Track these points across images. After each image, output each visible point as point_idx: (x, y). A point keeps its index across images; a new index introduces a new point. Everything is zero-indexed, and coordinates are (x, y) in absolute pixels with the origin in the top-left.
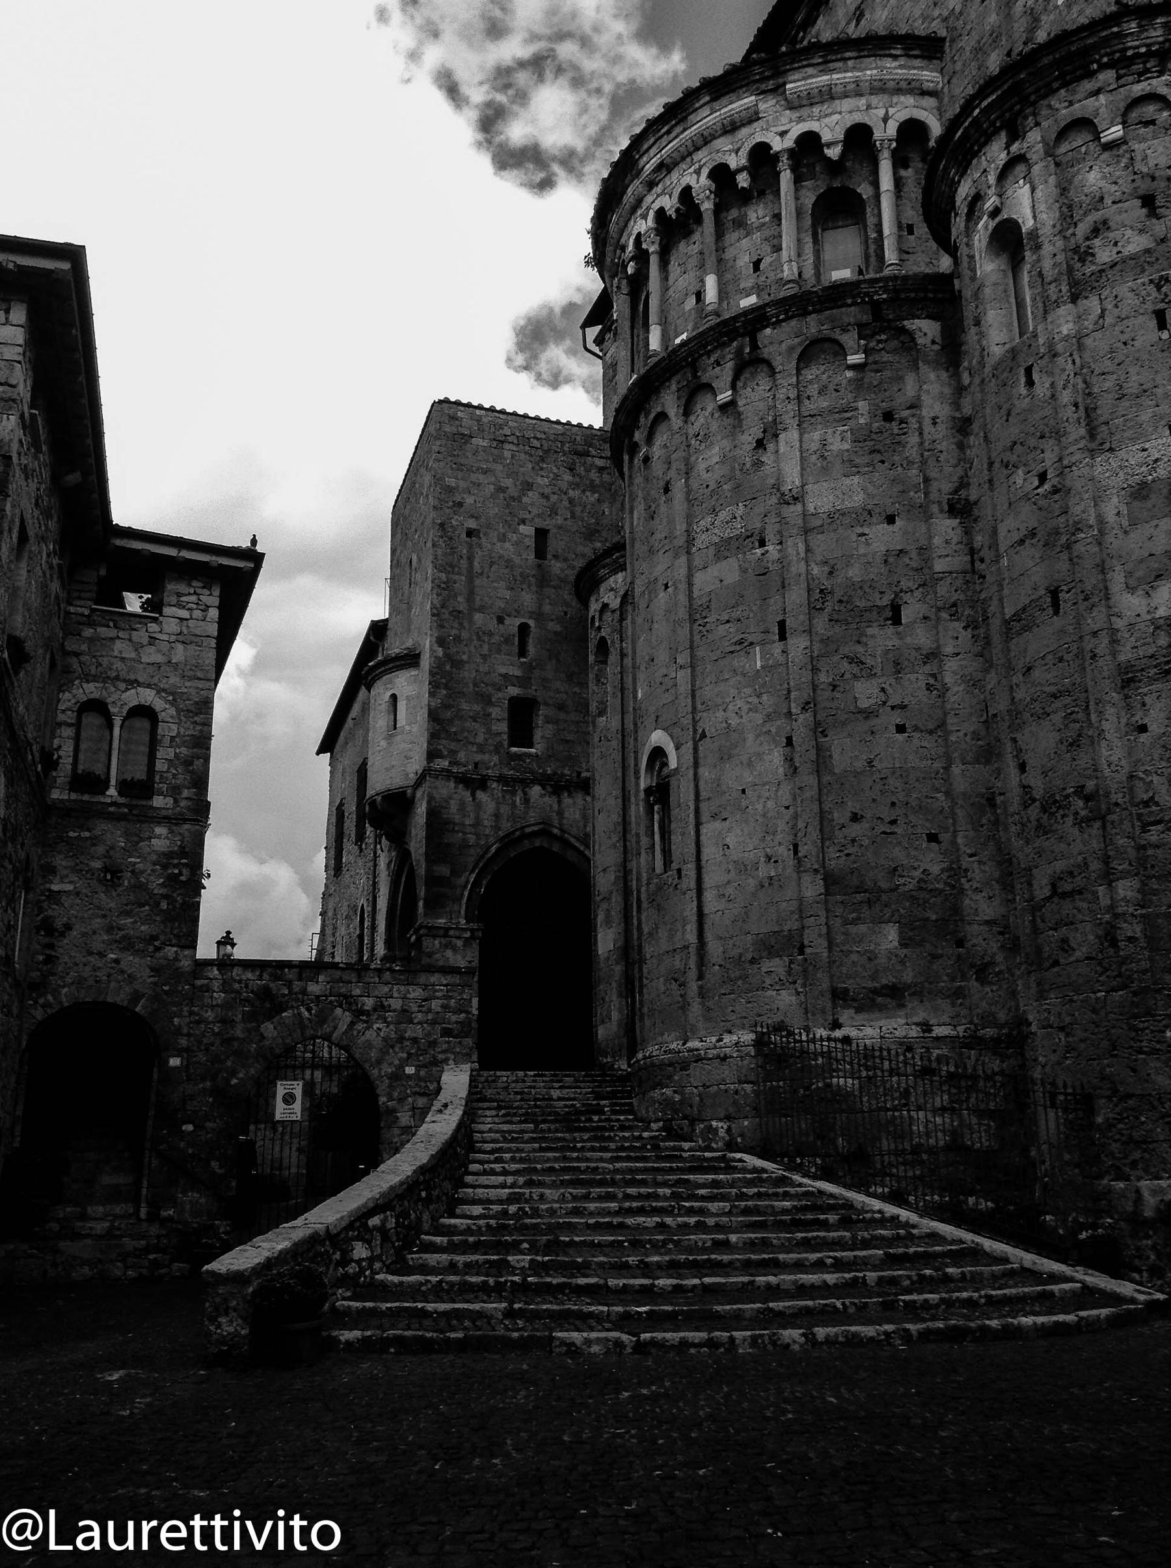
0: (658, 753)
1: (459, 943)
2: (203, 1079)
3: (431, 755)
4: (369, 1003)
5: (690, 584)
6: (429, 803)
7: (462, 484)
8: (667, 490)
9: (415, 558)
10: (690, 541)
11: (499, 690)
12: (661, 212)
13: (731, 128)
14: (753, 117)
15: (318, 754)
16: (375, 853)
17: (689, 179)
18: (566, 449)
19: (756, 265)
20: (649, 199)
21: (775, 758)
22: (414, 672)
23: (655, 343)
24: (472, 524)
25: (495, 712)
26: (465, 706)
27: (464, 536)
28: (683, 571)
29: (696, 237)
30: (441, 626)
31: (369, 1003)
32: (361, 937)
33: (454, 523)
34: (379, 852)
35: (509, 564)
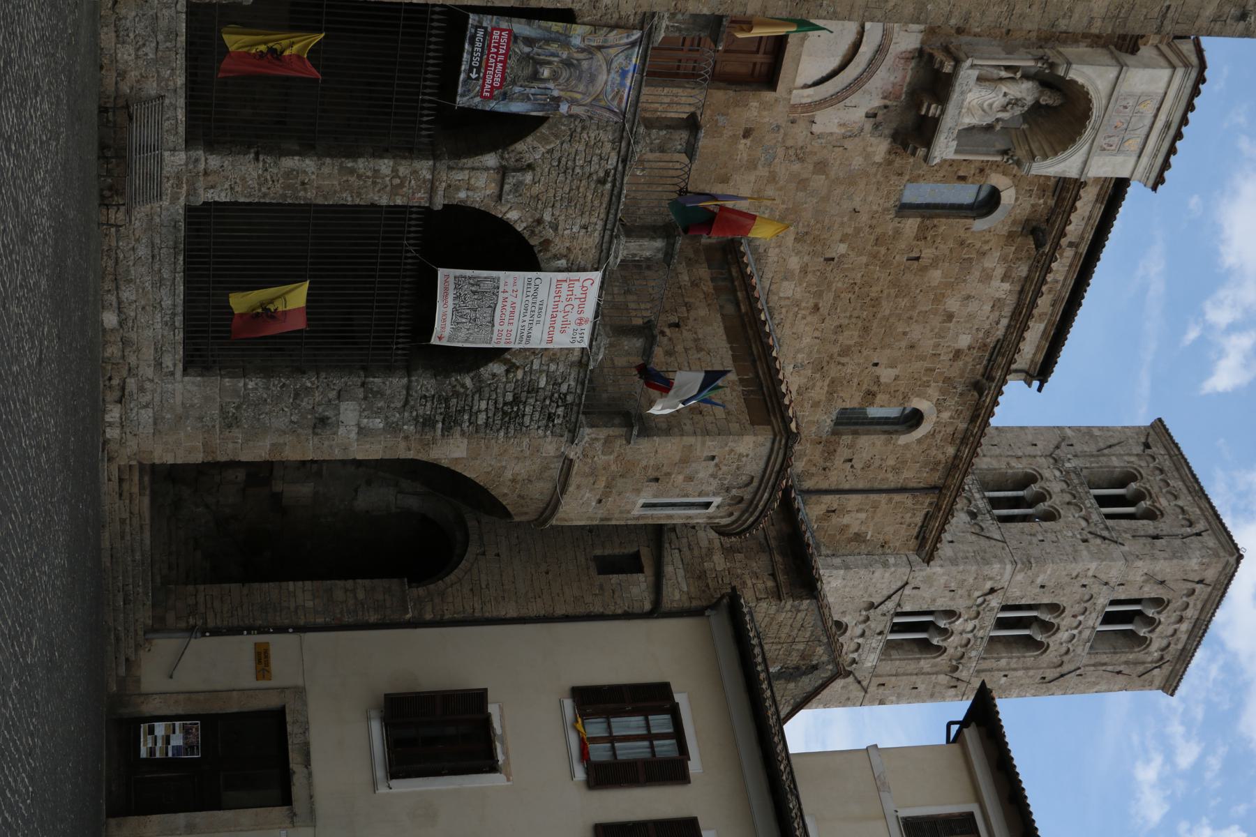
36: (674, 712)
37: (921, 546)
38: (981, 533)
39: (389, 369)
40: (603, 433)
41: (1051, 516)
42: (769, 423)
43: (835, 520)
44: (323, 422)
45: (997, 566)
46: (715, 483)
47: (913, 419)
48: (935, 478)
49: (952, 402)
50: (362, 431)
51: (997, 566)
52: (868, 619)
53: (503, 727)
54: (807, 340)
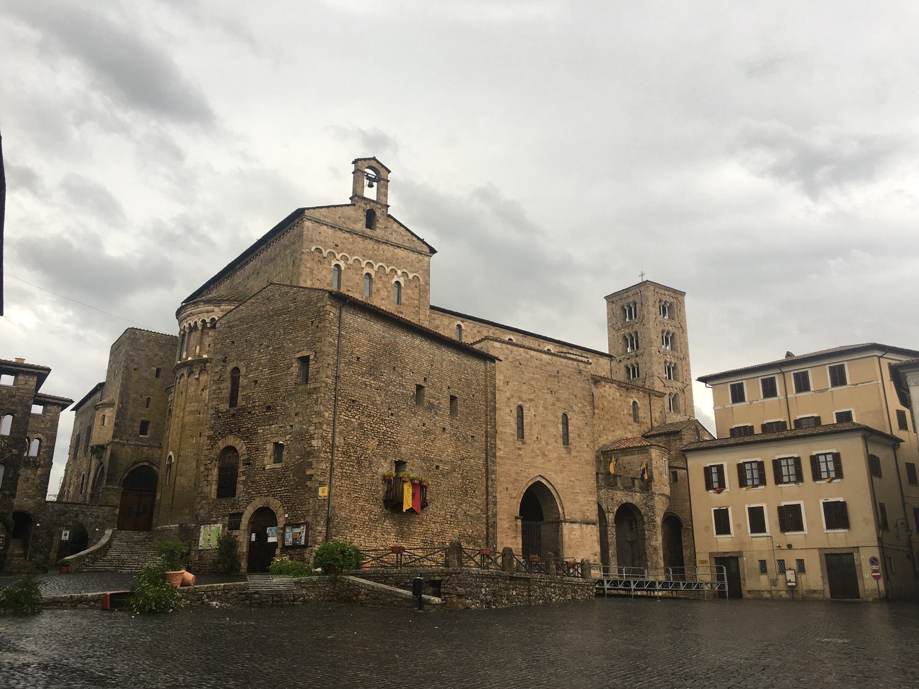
0: (170, 456)
1: (116, 493)
2: (45, 529)
3: (114, 437)
4: (88, 513)
5: (183, 419)
6: (111, 451)
7: (134, 354)
8: (182, 393)
9: (116, 371)
10: (185, 408)
11: (139, 418)
12: (190, 324)
13: (208, 312)
14: (213, 311)
15: (71, 411)
16: (91, 458)
17: (196, 320)
18: (170, 344)
19: (209, 345)
20: (188, 319)
21: (194, 464)
22: (112, 409)
23: (184, 356)
24: (136, 366)
25: (136, 425)
26: (126, 423)
27: (133, 370)
28: (182, 415)
29: (197, 332)
30: (122, 398)
31: (88, 513)
32: (82, 484)
33: (130, 366)
34: (92, 458)
35: (146, 379)
36: (711, 466)
37: (662, 396)
38: (642, 354)
39: (644, 534)
40: (653, 487)
41: (636, 333)
42: (648, 449)
43: (657, 419)
44: (655, 549)
45: (653, 351)
46: (661, 461)
47: (634, 403)
48: (647, 396)
49: (630, 394)
50: (657, 540)
51: (653, 351)
52: (668, 387)
53: (717, 507)
54: (620, 432)
